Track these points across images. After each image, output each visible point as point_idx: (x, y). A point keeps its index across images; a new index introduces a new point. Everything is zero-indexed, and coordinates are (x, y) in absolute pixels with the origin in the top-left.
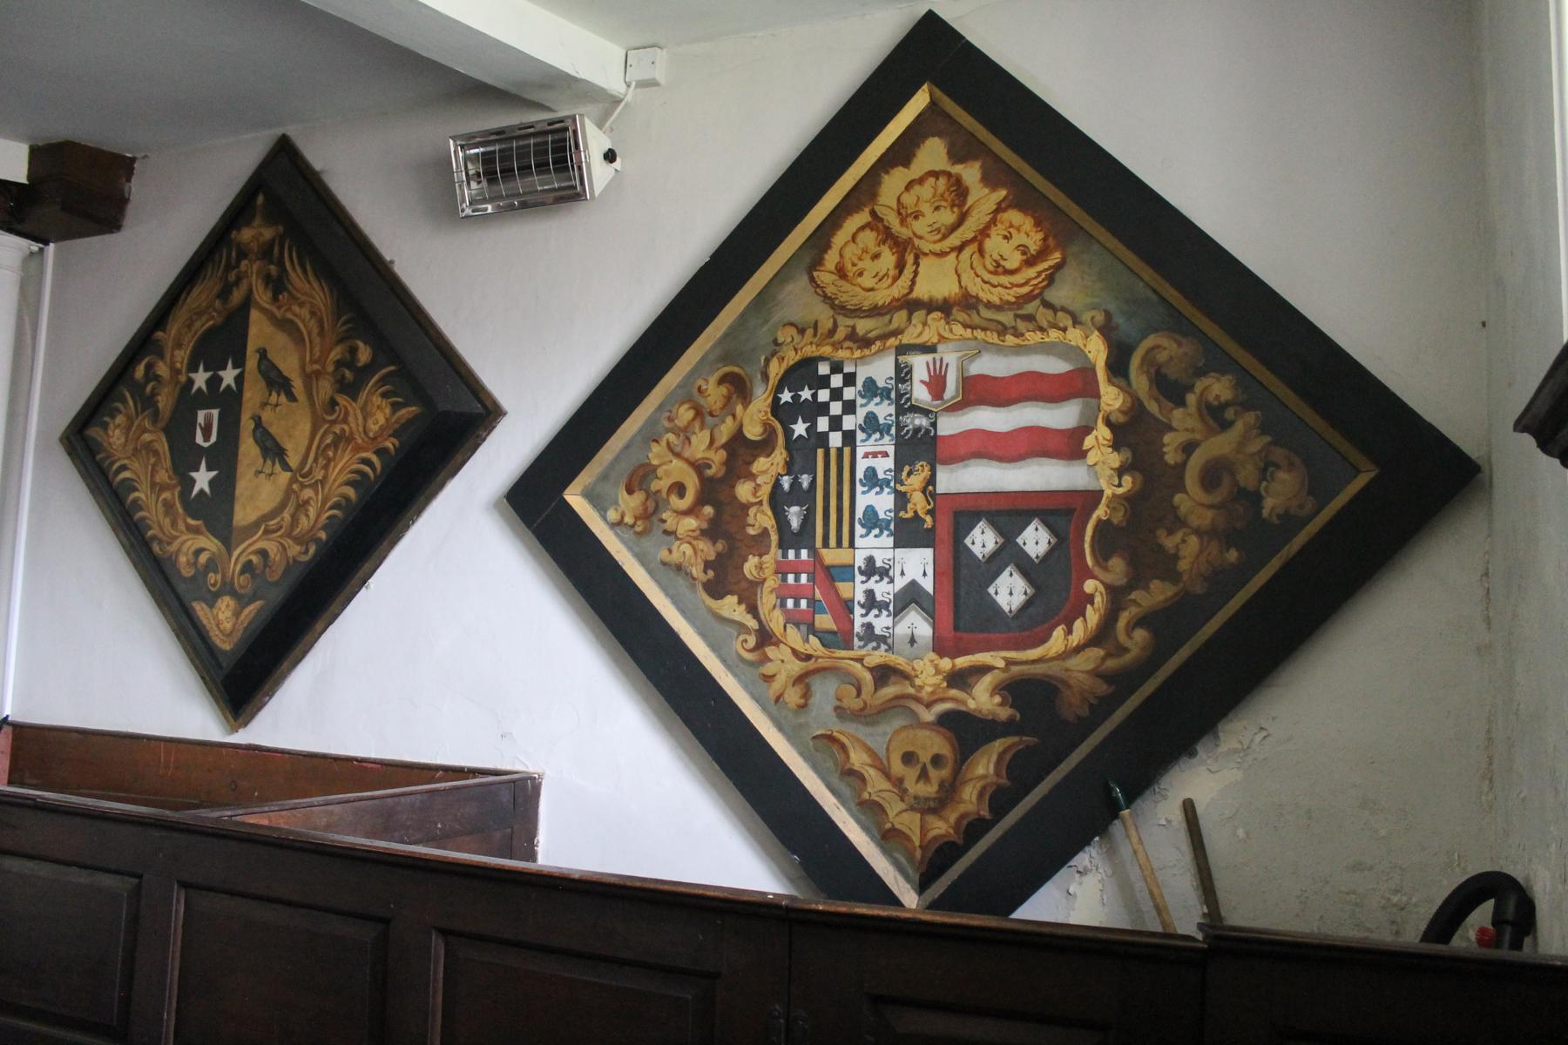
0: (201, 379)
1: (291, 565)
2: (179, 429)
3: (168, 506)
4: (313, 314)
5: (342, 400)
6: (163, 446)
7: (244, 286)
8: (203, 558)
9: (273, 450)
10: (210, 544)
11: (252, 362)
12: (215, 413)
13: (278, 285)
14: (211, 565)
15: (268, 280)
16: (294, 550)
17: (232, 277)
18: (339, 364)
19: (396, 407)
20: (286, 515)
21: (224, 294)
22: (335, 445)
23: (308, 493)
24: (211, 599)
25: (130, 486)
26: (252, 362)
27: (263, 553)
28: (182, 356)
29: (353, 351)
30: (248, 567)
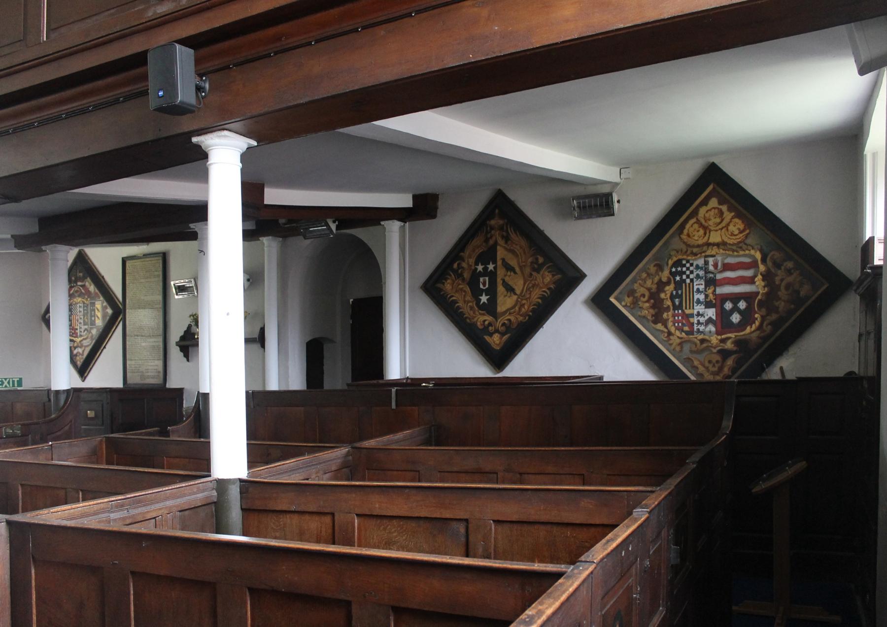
0: (480, 268)
1: (521, 324)
2: (473, 283)
3: (471, 308)
4: (521, 247)
5: (534, 273)
6: (468, 289)
7: (494, 238)
8: (486, 323)
9: (510, 289)
10: (489, 318)
11: (499, 263)
12: (487, 279)
13: (507, 239)
14: (490, 324)
15: (503, 237)
16: (521, 318)
17: (489, 236)
18: (532, 263)
19: (553, 275)
20: (517, 308)
21: (486, 241)
22: (534, 286)
23: (524, 302)
24: (491, 335)
25: (455, 302)
26: (499, 263)
27: (509, 320)
28: (472, 261)
29: (537, 259)
30: (504, 324)
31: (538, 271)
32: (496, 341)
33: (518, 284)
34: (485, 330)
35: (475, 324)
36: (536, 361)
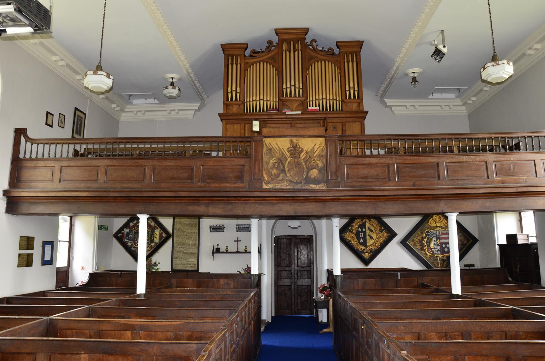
1: (376, 250)
9: (371, 238)
10: (364, 248)
11: (367, 228)
14: (364, 250)
24: (364, 253)
26: (367, 228)
28: (357, 227)
31: (382, 232)
32: (366, 256)
33: (374, 236)
34: (362, 252)
35: (358, 250)
36: (381, 262)
